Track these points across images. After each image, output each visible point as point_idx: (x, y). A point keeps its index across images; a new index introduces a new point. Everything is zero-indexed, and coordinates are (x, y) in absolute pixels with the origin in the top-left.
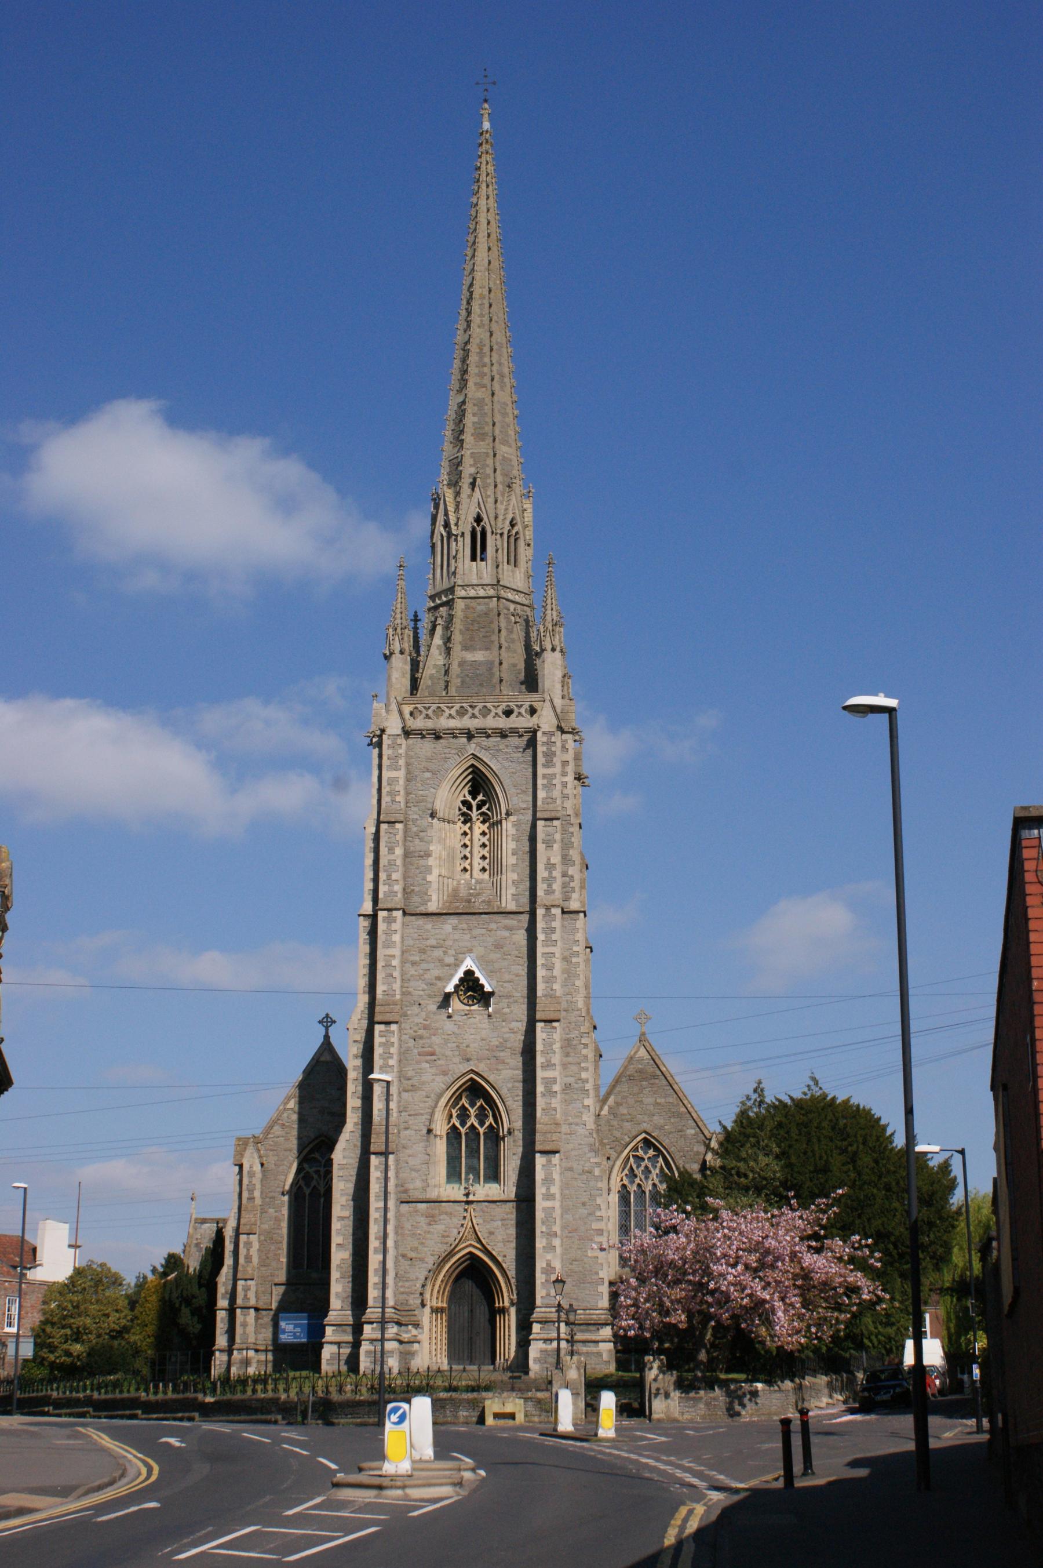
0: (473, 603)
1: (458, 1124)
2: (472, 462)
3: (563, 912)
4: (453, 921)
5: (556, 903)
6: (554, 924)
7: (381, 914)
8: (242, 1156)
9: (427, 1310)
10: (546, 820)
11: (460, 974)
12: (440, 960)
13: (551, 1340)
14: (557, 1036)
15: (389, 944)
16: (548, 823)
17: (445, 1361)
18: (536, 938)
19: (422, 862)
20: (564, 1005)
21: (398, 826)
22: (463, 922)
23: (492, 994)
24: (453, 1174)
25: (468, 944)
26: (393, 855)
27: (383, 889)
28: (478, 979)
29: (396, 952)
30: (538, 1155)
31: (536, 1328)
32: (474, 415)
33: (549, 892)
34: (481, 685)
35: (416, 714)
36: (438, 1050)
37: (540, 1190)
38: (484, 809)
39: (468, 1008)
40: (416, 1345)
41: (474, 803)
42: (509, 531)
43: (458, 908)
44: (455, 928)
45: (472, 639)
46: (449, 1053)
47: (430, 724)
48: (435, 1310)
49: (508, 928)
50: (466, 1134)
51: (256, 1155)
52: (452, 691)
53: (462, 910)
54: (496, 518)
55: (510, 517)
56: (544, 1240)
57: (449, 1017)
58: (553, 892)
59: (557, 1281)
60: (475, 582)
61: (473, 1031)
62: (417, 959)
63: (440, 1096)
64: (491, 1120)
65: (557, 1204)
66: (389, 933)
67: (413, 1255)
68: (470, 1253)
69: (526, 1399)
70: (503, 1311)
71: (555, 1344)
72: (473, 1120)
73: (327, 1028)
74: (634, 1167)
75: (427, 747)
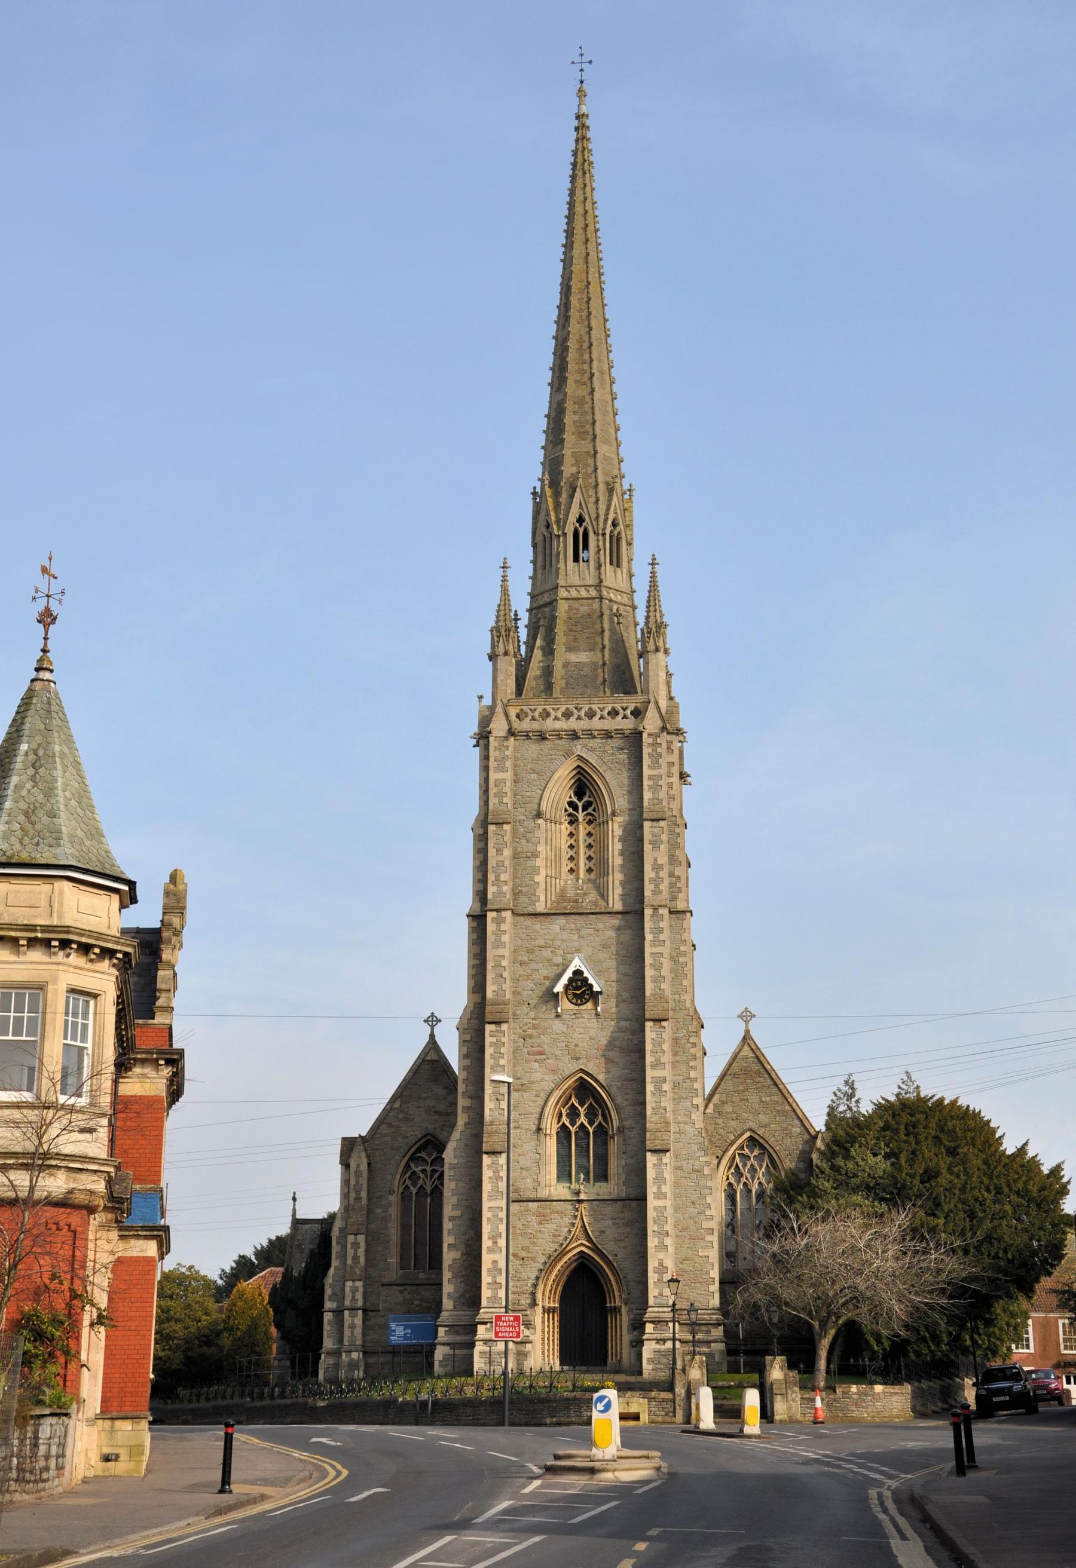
0: (576, 604)
1: (567, 1124)
2: (573, 462)
3: (671, 912)
4: (561, 921)
5: (663, 903)
6: (662, 924)
7: (491, 915)
8: (349, 1156)
9: (539, 1310)
10: (652, 820)
11: (569, 974)
13: (664, 1341)
14: (667, 1035)
15: (499, 944)
16: (655, 824)
17: (557, 1362)
18: (644, 939)
19: (530, 863)
20: (672, 1004)
21: (506, 827)
23: (600, 993)
24: (564, 1174)
25: (576, 944)
26: (500, 856)
27: (491, 890)
28: (586, 979)
29: (506, 952)
30: (648, 1154)
31: (649, 1328)
32: (575, 413)
33: (657, 892)
34: (585, 686)
35: (522, 716)
37: (651, 1190)
38: (590, 810)
40: (529, 1346)
41: (580, 805)
42: (611, 532)
43: (565, 908)
45: (576, 640)
47: (536, 726)
48: (547, 1311)
50: (576, 1133)
51: (363, 1155)
52: (556, 693)
53: (566, 910)
54: (597, 518)
55: (611, 517)
56: (656, 1239)
57: (558, 1016)
58: (661, 892)
59: (672, 1280)
60: (578, 583)
61: (582, 1030)
62: (526, 959)
64: (600, 1118)
65: (668, 1203)
66: (500, 933)
67: (524, 1254)
68: (582, 1252)
69: (650, 1399)
70: (616, 1310)
71: (669, 1345)
72: (583, 1119)
73: (432, 1027)
74: (740, 1166)
75: (532, 749)
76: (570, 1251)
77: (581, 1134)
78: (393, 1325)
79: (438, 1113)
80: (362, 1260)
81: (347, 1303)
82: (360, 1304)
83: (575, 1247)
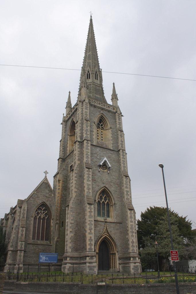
11: (104, 161)
12: (97, 157)
22: (101, 149)
36: (96, 180)
39: (103, 170)
44: (99, 150)
46: (99, 181)
49: (111, 153)
63: (97, 192)
76: (103, 236)
77: (103, 204)
78: (41, 256)
79: (46, 197)
80: (24, 235)
81: (19, 248)
82: (23, 249)
83: (104, 235)
